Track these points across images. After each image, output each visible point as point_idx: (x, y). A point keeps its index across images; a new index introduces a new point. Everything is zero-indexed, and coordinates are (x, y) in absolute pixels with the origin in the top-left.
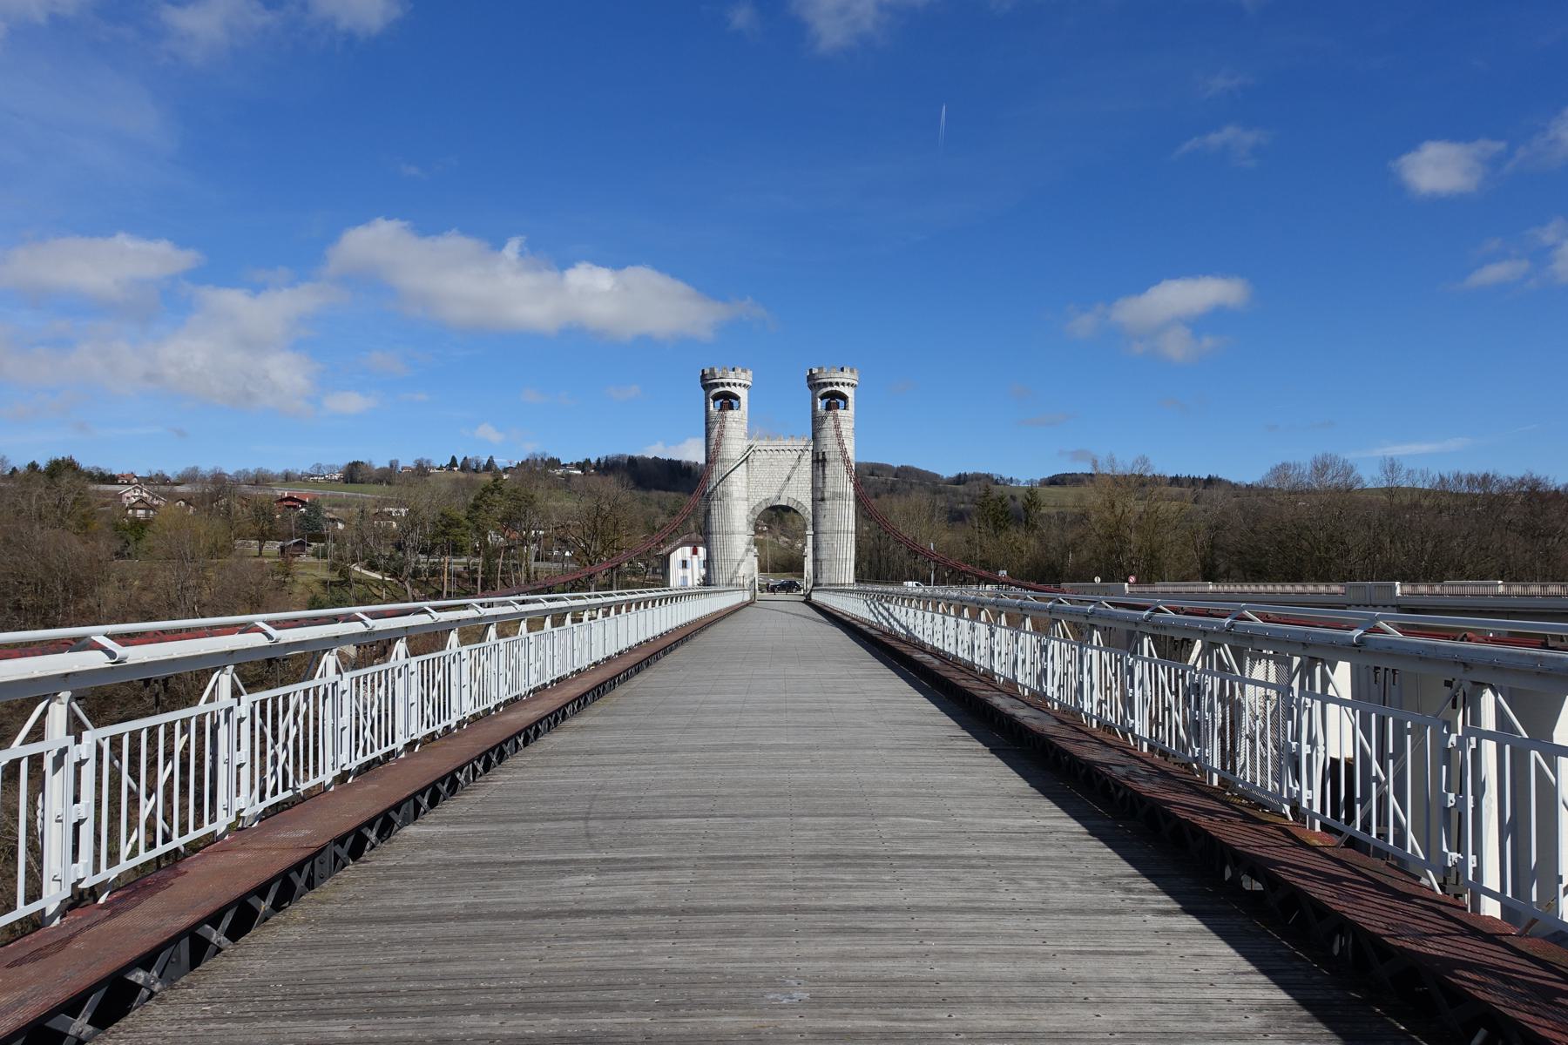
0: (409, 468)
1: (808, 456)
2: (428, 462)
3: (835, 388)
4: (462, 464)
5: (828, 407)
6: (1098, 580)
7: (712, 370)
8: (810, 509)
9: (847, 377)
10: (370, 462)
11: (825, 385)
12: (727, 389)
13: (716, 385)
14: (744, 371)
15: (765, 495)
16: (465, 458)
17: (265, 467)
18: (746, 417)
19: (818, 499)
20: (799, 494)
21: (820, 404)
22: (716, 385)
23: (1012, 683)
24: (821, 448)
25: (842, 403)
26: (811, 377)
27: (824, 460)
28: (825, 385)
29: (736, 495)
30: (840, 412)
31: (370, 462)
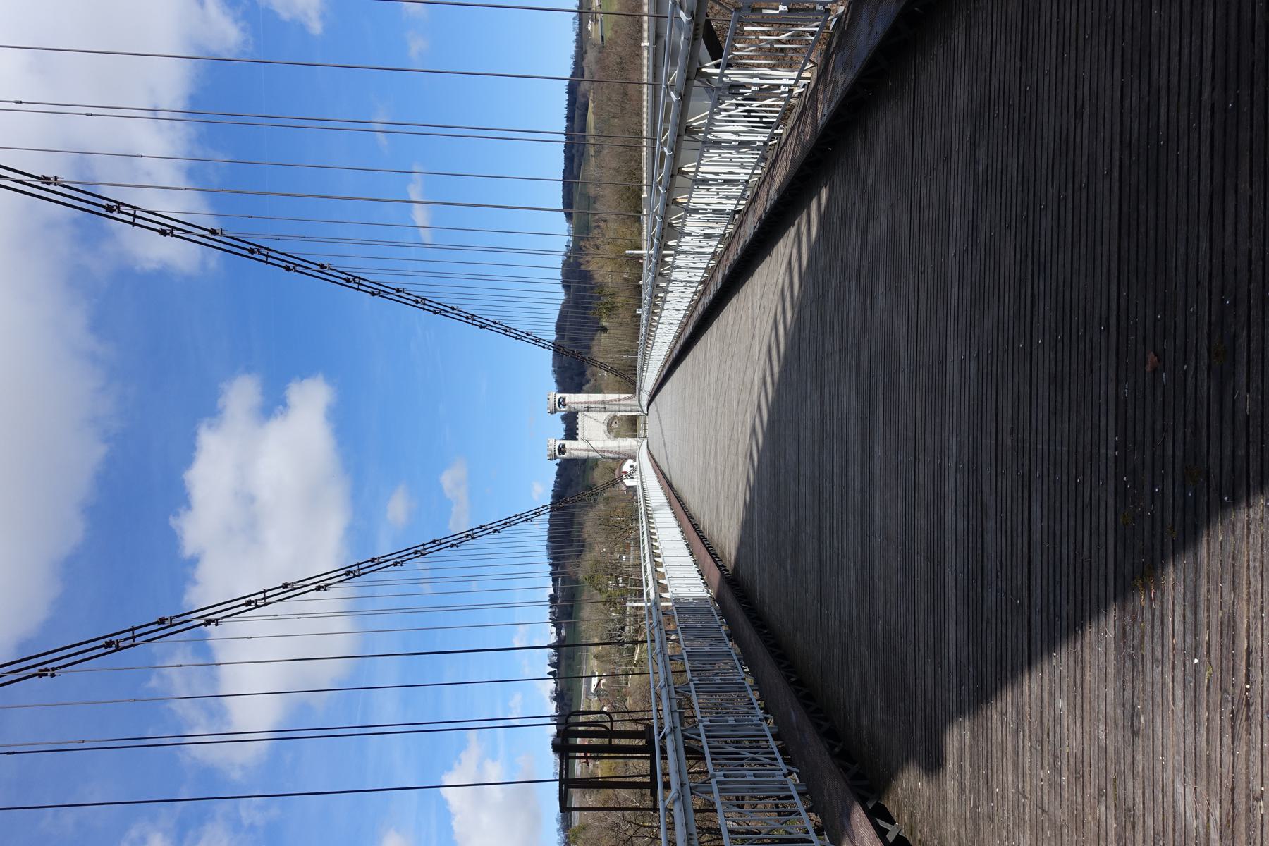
0: (557, 706)
1: (586, 413)
2: (552, 692)
3: (557, 402)
4: (553, 667)
5: (564, 405)
6: (641, 283)
7: (548, 455)
8: (609, 413)
9: (552, 397)
10: (552, 736)
11: (555, 407)
12: (556, 449)
13: (555, 454)
14: (549, 441)
15: (603, 433)
16: (549, 665)
17: (555, 816)
18: (568, 441)
19: (605, 410)
20: (603, 417)
21: (563, 409)
22: (555, 454)
23: (707, 270)
24: (583, 409)
25: (561, 400)
26: (551, 413)
27: (588, 407)
28: (555, 407)
29: (602, 446)
30: (567, 401)
31: (552, 736)
